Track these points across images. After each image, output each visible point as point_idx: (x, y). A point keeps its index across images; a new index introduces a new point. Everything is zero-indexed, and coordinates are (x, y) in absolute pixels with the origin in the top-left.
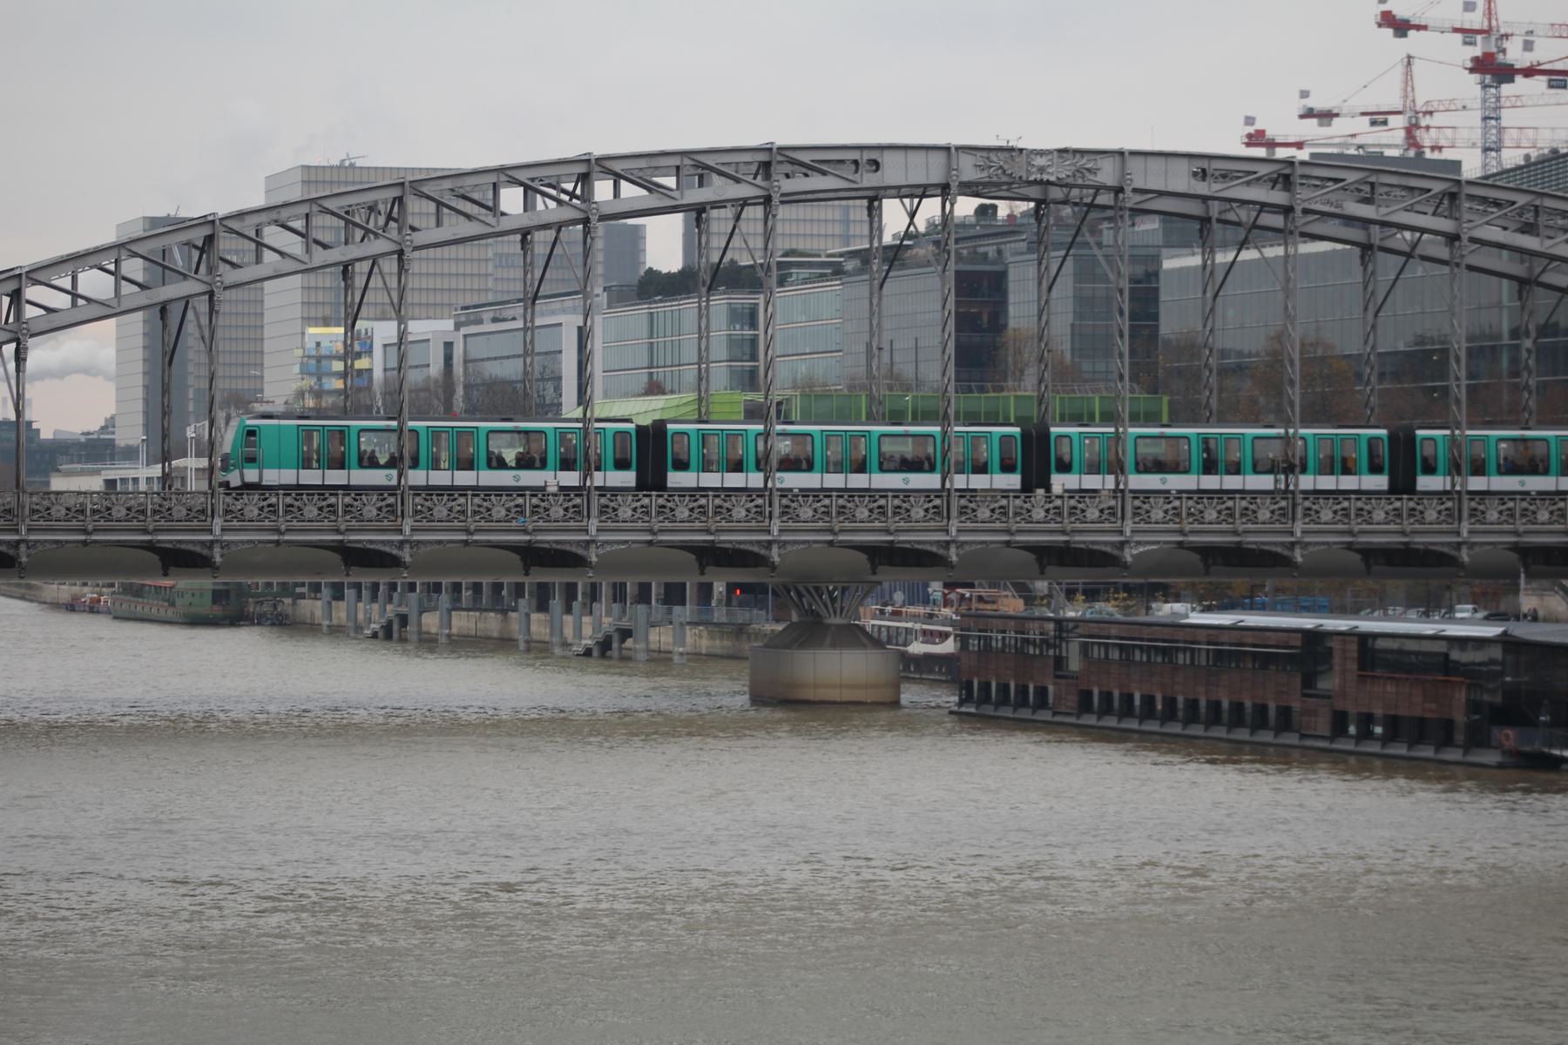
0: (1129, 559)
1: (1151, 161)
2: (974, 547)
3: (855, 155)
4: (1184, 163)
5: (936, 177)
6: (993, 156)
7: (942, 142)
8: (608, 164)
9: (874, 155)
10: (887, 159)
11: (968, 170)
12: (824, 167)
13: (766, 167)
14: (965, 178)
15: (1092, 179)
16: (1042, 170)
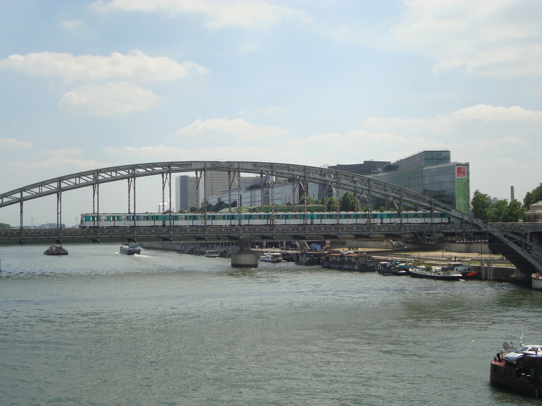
0: (241, 238)
1: (244, 163)
2: (210, 237)
3: (187, 163)
4: (251, 164)
5: (202, 167)
6: (213, 163)
7: (203, 160)
8: (138, 166)
9: (190, 163)
10: (193, 164)
11: (208, 166)
12: (181, 166)
13: (169, 165)
14: (208, 167)
15: (233, 167)
16: (223, 165)
